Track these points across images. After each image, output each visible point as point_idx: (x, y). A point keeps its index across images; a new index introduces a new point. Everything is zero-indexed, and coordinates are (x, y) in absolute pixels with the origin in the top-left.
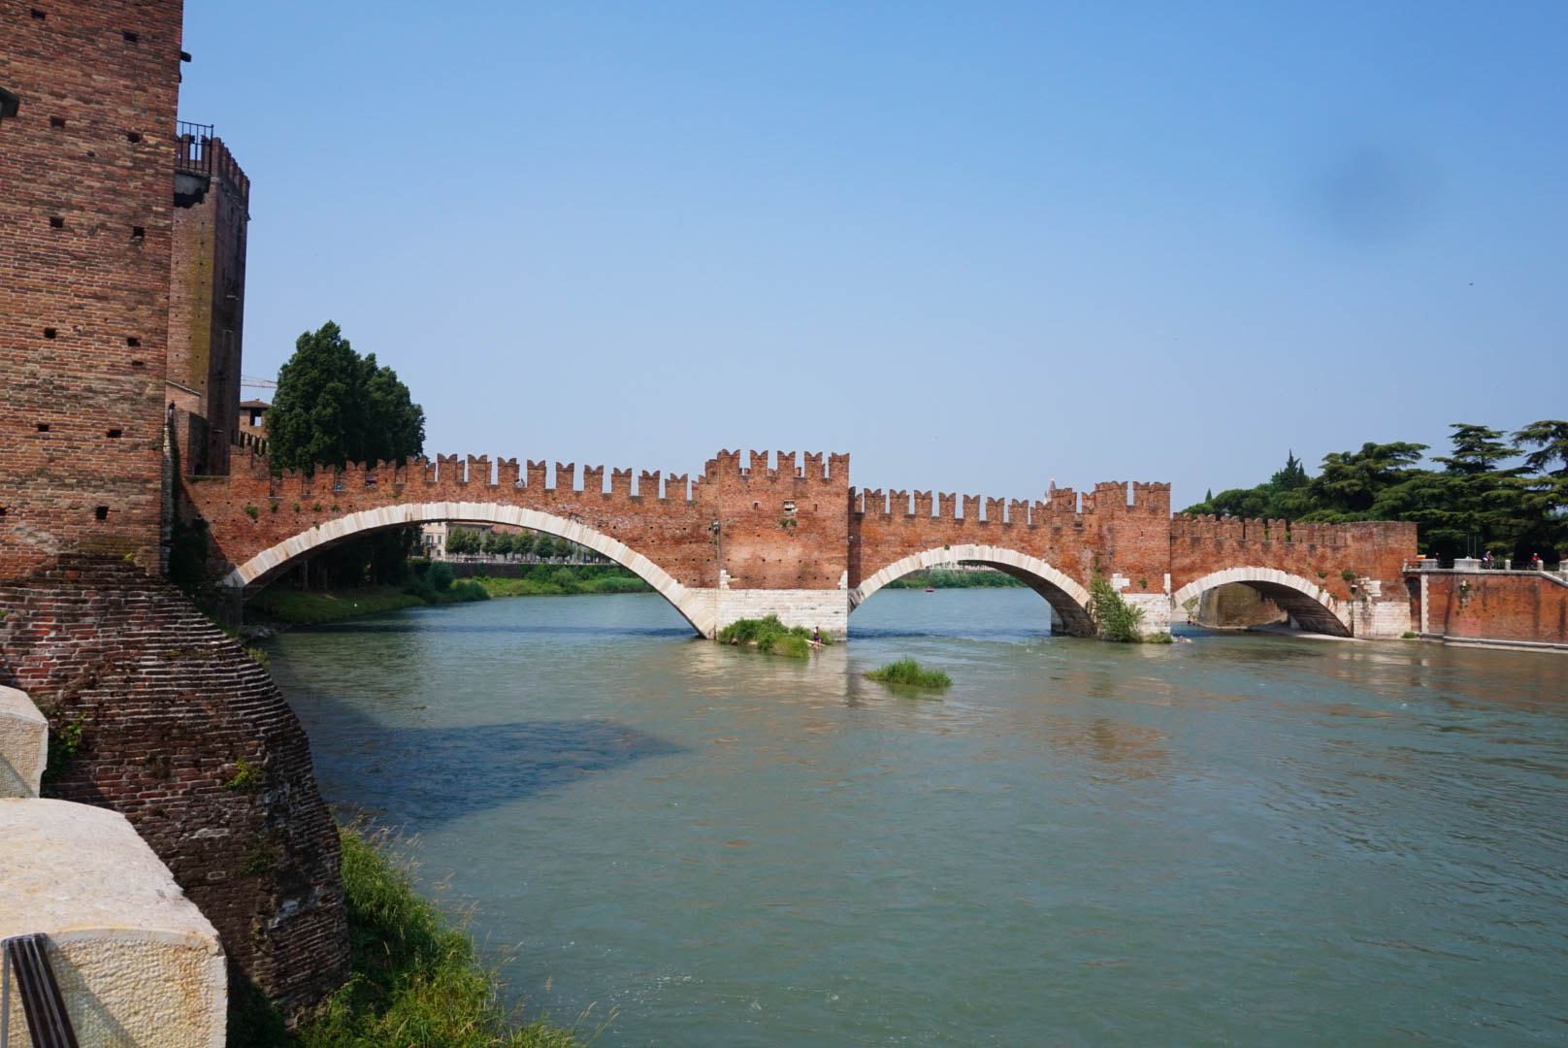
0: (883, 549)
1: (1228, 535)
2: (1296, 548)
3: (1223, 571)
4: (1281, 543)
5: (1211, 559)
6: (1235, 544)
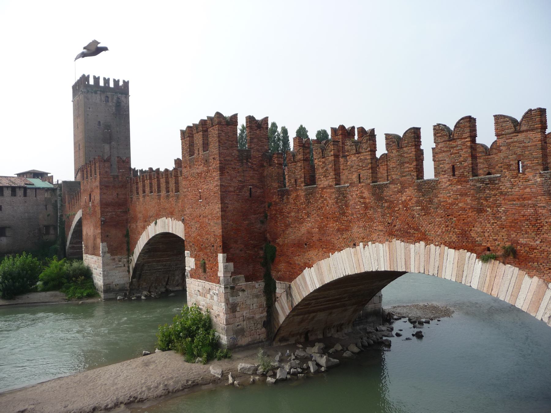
0: (140, 224)
1: (354, 177)
2: (505, 186)
3: (351, 250)
4: (462, 180)
5: (333, 226)
6: (366, 194)
